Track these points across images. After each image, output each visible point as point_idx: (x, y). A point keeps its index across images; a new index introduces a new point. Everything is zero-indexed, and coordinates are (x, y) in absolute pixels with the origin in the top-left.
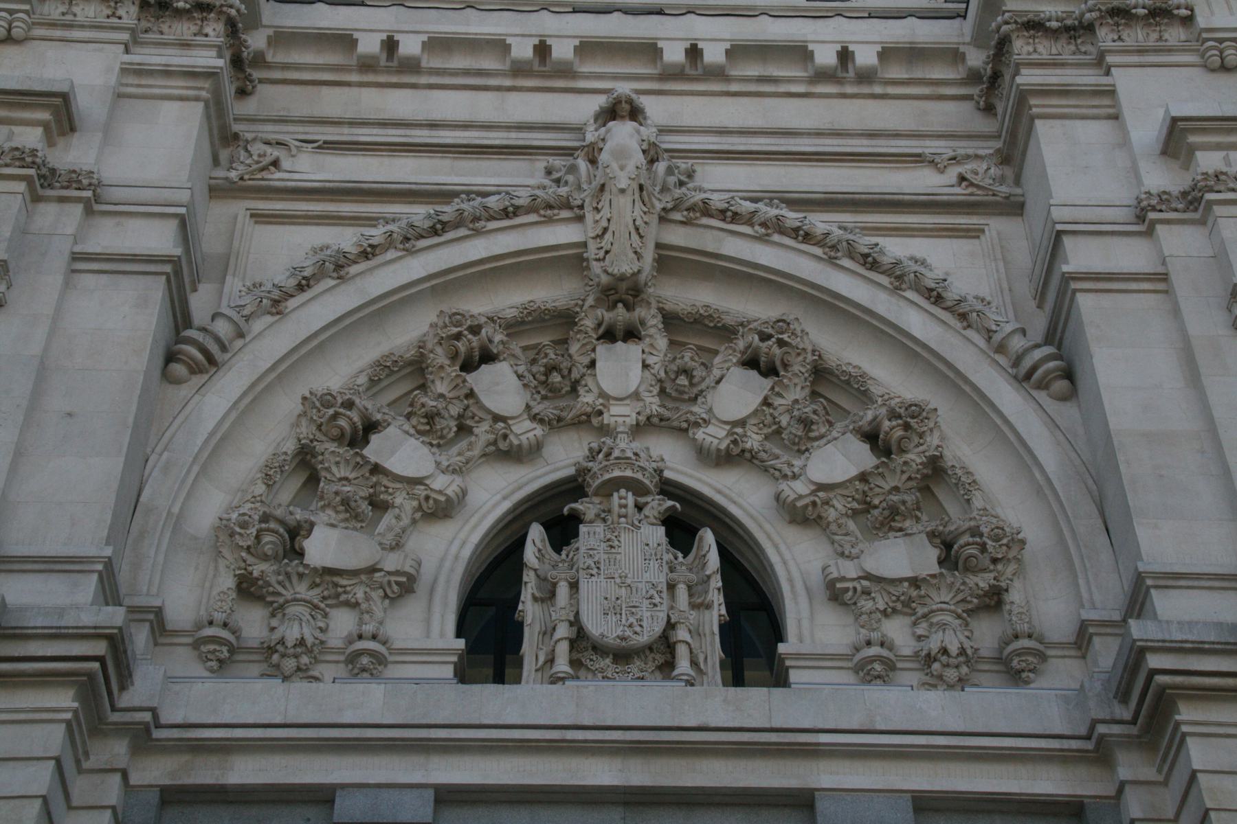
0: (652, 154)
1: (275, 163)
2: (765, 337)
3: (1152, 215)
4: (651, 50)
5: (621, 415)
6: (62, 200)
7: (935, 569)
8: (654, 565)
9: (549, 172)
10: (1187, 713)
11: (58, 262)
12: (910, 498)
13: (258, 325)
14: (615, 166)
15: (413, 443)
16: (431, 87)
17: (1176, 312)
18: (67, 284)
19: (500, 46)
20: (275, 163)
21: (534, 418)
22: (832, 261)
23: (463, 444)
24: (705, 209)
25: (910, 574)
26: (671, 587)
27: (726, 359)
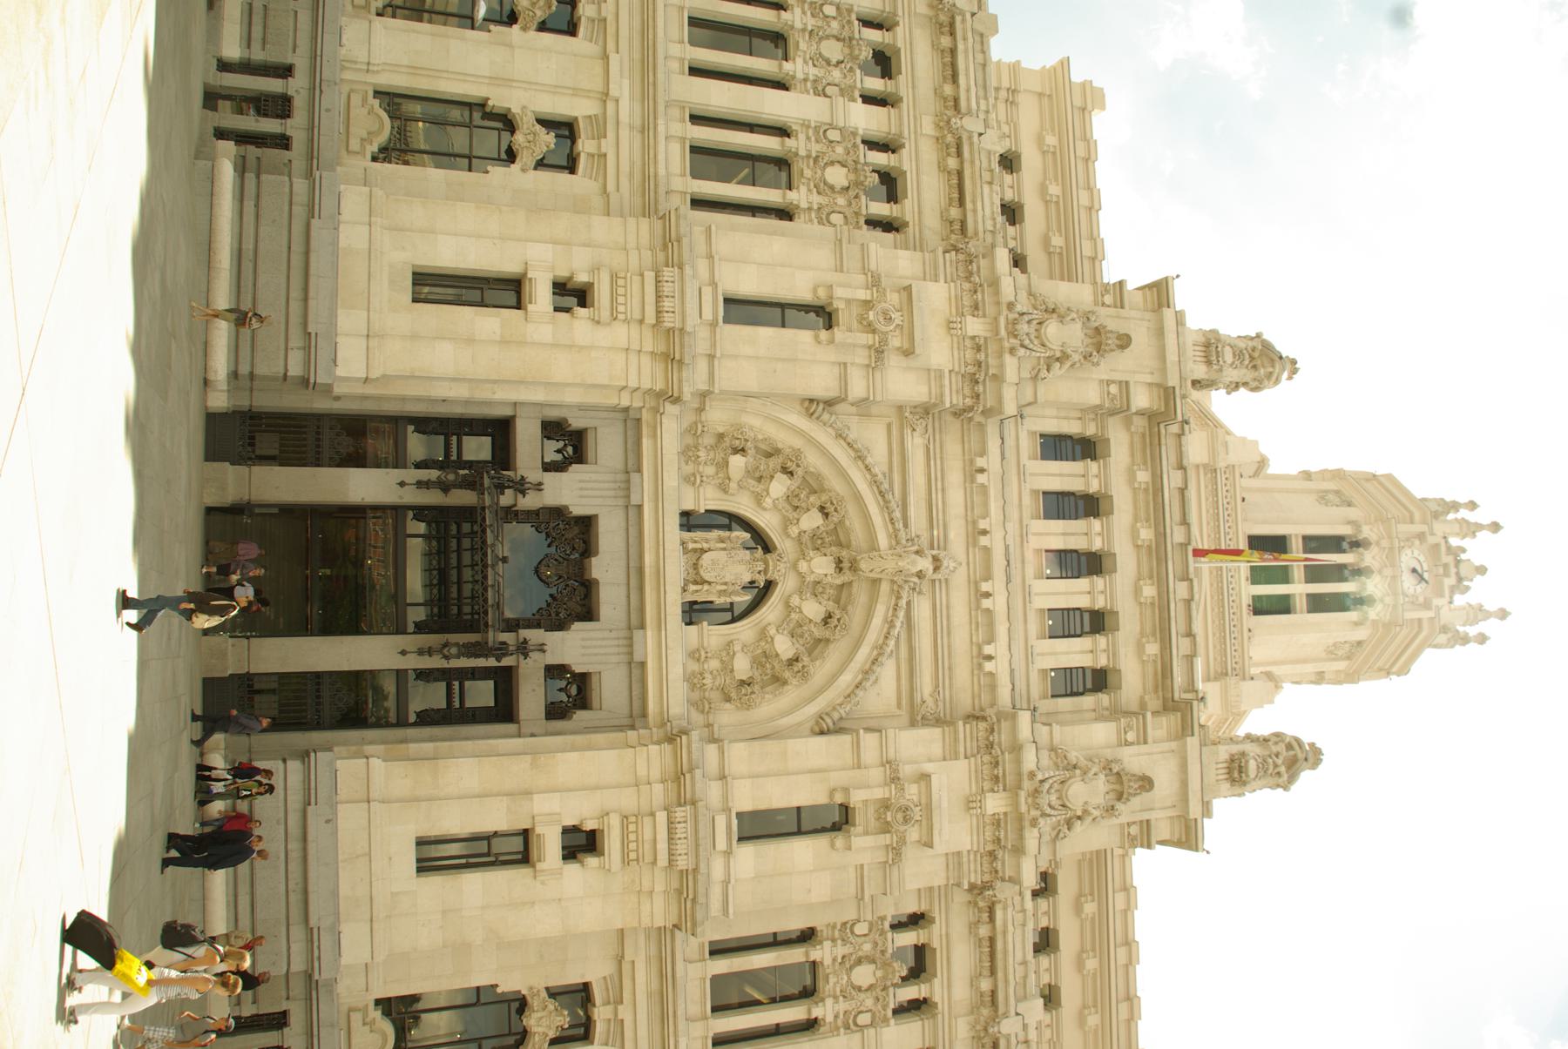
0: (920, 574)
2: (839, 620)
4: (988, 577)
5: (803, 566)
6: (870, 356)
8: (733, 577)
9: (918, 537)
10: (667, 747)
11: (842, 359)
12: (769, 671)
13: (830, 430)
15: (785, 490)
16: (965, 489)
17: (844, 769)
18: (833, 363)
19: (985, 515)
20: (914, 430)
21: (800, 533)
23: (788, 507)
24: (899, 598)
26: (726, 584)
27: (831, 606)
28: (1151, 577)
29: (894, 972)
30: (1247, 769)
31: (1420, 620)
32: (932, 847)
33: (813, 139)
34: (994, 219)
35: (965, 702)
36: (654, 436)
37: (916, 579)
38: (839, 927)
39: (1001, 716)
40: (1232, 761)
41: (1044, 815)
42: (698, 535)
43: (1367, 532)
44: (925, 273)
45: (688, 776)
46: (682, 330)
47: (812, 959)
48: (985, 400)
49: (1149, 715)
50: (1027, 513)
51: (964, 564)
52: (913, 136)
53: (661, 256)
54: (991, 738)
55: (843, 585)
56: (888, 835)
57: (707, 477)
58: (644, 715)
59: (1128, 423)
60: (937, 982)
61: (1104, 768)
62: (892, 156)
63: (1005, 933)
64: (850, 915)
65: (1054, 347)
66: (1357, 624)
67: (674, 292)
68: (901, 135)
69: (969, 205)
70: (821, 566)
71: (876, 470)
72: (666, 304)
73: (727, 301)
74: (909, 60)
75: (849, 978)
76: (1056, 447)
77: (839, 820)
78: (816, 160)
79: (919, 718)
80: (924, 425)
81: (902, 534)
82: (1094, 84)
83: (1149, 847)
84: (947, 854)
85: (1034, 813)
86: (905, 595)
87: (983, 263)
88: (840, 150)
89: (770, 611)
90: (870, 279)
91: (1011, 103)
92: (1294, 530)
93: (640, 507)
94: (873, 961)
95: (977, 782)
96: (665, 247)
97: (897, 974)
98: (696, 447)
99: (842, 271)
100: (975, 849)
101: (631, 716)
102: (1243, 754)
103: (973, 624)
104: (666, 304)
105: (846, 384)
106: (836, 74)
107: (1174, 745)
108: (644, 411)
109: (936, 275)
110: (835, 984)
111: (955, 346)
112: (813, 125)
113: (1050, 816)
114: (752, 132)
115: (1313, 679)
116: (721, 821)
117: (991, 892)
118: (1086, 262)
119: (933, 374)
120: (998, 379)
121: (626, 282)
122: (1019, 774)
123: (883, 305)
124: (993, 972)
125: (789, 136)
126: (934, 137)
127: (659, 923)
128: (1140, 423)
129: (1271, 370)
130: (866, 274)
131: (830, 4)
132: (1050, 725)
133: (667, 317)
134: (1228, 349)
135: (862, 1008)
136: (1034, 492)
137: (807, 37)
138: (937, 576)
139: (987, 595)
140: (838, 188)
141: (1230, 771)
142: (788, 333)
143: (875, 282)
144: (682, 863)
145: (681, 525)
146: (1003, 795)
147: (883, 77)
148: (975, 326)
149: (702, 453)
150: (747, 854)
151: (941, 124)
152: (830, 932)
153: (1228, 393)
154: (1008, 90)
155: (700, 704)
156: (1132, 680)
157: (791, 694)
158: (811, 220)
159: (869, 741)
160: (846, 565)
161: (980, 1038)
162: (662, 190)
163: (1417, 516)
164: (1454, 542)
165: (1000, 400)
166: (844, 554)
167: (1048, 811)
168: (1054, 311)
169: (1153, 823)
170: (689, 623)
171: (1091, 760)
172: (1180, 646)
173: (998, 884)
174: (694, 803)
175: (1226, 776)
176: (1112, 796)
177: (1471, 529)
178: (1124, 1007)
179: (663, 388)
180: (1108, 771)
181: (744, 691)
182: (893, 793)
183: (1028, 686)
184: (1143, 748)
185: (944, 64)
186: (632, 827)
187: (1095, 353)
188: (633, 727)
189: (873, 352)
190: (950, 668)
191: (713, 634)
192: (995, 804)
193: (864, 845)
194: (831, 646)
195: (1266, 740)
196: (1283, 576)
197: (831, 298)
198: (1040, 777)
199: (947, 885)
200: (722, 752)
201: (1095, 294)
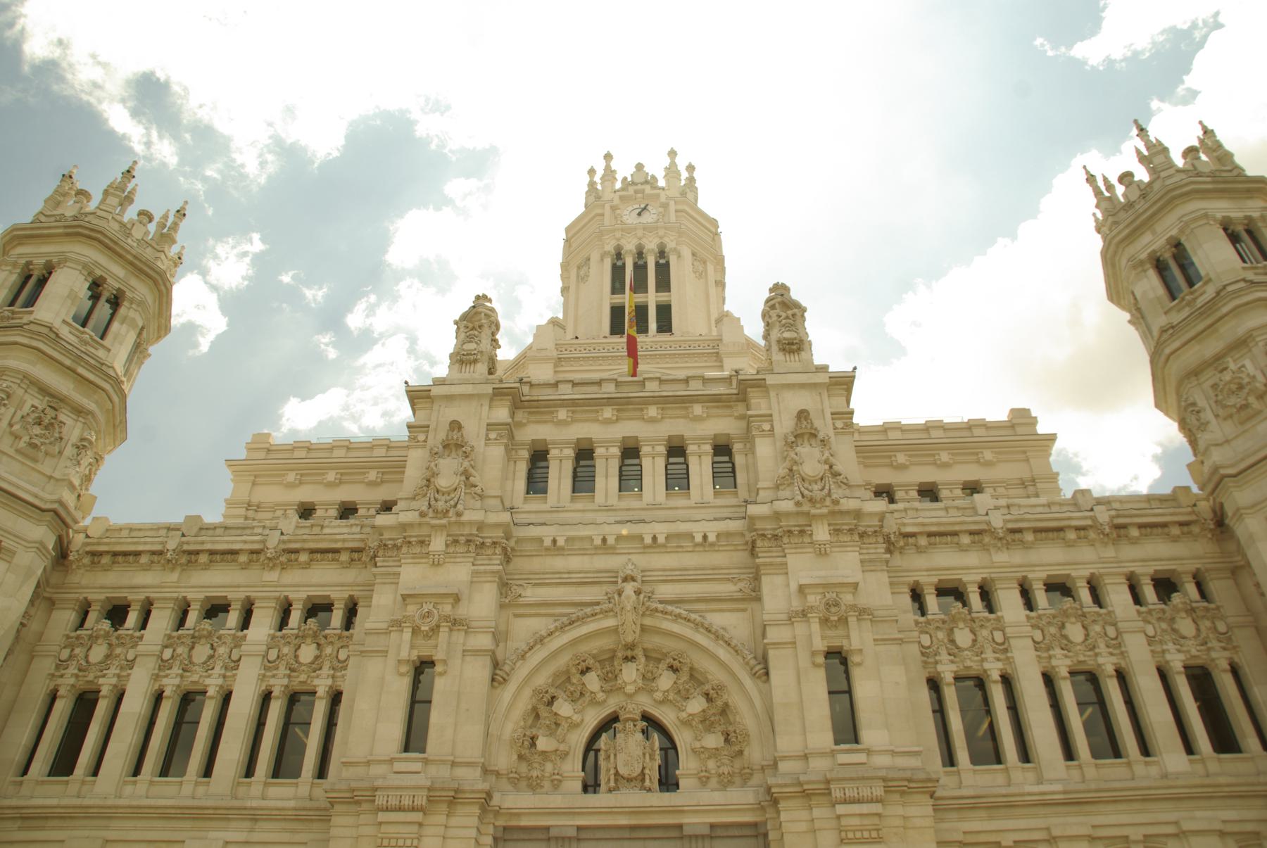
0: (638, 593)
1: (520, 595)
2: (674, 659)
3: (793, 620)
5: (630, 689)
6: (459, 630)
7: (722, 744)
9: (607, 594)
10: (782, 805)
11: (459, 655)
14: (626, 602)
15: (566, 703)
17: (796, 656)
18: (463, 660)
19: (591, 539)
20: (520, 595)
21: (603, 691)
22: (697, 630)
23: (580, 701)
24: (656, 610)
25: (715, 747)
27: (663, 666)
28: (642, 410)
29: (959, 613)
30: (791, 339)
31: (676, 211)
32: (857, 584)
33: (275, 672)
34: (352, 525)
35: (741, 557)
36: (518, 815)
37: (642, 596)
38: (925, 659)
39: (751, 528)
40: (784, 350)
41: (829, 494)
42: (603, 778)
43: (610, 247)
44: (392, 583)
45: (806, 787)
46: (429, 789)
47: (952, 681)
48: (497, 537)
49: (749, 413)
50: (590, 506)
51: (630, 557)
52: (278, 589)
53: (365, 806)
54: (770, 536)
55: (646, 656)
56: (849, 619)
57: (555, 769)
58: (755, 825)
59: (520, 425)
60: (965, 578)
61: (792, 447)
62: (294, 606)
63: (924, 525)
64: (915, 649)
65: (458, 481)
66: (679, 256)
67: (396, 796)
68: (277, 599)
69: (339, 545)
70: (630, 674)
71: (552, 627)
72: (406, 803)
73: (406, 749)
74: (215, 589)
75: (966, 650)
76: (536, 483)
77: (838, 659)
78: (292, 670)
79: (754, 594)
80: (516, 587)
81: (606, 606)
82: (249, 441)
83: (852, 413)
84: (863, 571)
85: (828, 502)
86: (654, 605)
87: (386, 535)
88: (286, 650)
89: (667, 717)
90: (394, 629)
91: (259, 507)
92: (607, 300)
93: (579, 828)
94: (952, 630)
95: (804, 548)
96: (358, 803)
97: (961, 610)
98: (529, 778)
99: (387, 652)
100: (858, 549)
101: (757, 836)
102: (779, 341)
103: (679, 549)
104: (406, 803)
105: (478, 651)
106: (222, 650)
107: (772, 394)
108: (497, 824)
109: (394, 574)
110: (972, 661)
111: (452, 560)
112: (263, 672)
113: (830, 490)
114: (264, 724)
115: (721, 289)
116: (843, 758)
117: (892, 536)
118: (391, 453)
119: (475, 579)
120: (481, 526)
121: (386, 838)
122: (798, 514)
123: (416, 618)
124: (955, 534)
125: (271, 693)
126: (280, 573)
127: (929, 810)
128: (520, 415)
129: (483, 314)
130: (391, 631)
131: (162, 653)
132: (758, 489)
133: (418, 802)
134: (465, 347)
135: (990, 638)
136: (573, 499)
137: (188, 674)
138: (639, 578)
139: (655, 538)
140: (317, 652)
141: (791, 352)
142: (436, 699)
143: (398, 624)
144: (879, 791)
145: (595, 792)
146: (814, 526)
147: (228, 611)
148: (438, 544)
149: (535, 773)
150: (869, 736)
151: (271, 565)
152: (930, 666)
153: (500, 347)
154: (247, 510)
155: (745, 777)
156: (722, 425)
157: (735, 698)
158: (343, 676)
159: (773, 635)
160: (629, 653)
161: (1008, 543)
162: (308, 804)
163: (599, 211)
164: (618, 185)
165: (497, 525)
166: (620, 655)
167: (826, 491)
168: (428, 480)
169: (833, 410)
170: (677, 786)
171: (785, 458)
172: (696, 388)
173: (885, 530)
174: (828, 782)
175: (796, 354)
176: (813, 442)
177: (609, 174)
178: (977, 432)
179: (478, 806)
180: (794, 445)
181: (734, 739)
182: (815, 615)
183: (727, 507)
184: (776, 417)
185: (222, 561)
186: (850, 835)
187: (464, 449)
188: (766, 835)
189: (455, 628)
190: (713, 569)
191: (687, 765)
192: (821, 533)
193: (858, 638)
194: (696, 666)
195: (768, 324)
196: (641, 311)
197: (408, 661)
198: (799, 498)
199: (888, 571)
200: (784, 758)
201: (417, 447)
